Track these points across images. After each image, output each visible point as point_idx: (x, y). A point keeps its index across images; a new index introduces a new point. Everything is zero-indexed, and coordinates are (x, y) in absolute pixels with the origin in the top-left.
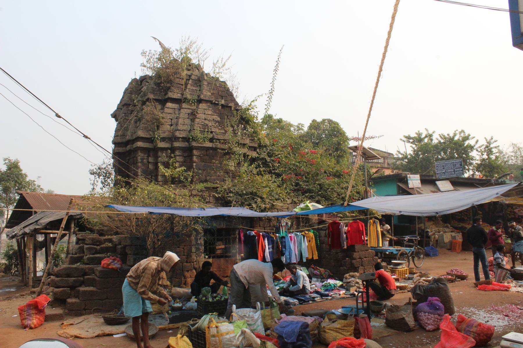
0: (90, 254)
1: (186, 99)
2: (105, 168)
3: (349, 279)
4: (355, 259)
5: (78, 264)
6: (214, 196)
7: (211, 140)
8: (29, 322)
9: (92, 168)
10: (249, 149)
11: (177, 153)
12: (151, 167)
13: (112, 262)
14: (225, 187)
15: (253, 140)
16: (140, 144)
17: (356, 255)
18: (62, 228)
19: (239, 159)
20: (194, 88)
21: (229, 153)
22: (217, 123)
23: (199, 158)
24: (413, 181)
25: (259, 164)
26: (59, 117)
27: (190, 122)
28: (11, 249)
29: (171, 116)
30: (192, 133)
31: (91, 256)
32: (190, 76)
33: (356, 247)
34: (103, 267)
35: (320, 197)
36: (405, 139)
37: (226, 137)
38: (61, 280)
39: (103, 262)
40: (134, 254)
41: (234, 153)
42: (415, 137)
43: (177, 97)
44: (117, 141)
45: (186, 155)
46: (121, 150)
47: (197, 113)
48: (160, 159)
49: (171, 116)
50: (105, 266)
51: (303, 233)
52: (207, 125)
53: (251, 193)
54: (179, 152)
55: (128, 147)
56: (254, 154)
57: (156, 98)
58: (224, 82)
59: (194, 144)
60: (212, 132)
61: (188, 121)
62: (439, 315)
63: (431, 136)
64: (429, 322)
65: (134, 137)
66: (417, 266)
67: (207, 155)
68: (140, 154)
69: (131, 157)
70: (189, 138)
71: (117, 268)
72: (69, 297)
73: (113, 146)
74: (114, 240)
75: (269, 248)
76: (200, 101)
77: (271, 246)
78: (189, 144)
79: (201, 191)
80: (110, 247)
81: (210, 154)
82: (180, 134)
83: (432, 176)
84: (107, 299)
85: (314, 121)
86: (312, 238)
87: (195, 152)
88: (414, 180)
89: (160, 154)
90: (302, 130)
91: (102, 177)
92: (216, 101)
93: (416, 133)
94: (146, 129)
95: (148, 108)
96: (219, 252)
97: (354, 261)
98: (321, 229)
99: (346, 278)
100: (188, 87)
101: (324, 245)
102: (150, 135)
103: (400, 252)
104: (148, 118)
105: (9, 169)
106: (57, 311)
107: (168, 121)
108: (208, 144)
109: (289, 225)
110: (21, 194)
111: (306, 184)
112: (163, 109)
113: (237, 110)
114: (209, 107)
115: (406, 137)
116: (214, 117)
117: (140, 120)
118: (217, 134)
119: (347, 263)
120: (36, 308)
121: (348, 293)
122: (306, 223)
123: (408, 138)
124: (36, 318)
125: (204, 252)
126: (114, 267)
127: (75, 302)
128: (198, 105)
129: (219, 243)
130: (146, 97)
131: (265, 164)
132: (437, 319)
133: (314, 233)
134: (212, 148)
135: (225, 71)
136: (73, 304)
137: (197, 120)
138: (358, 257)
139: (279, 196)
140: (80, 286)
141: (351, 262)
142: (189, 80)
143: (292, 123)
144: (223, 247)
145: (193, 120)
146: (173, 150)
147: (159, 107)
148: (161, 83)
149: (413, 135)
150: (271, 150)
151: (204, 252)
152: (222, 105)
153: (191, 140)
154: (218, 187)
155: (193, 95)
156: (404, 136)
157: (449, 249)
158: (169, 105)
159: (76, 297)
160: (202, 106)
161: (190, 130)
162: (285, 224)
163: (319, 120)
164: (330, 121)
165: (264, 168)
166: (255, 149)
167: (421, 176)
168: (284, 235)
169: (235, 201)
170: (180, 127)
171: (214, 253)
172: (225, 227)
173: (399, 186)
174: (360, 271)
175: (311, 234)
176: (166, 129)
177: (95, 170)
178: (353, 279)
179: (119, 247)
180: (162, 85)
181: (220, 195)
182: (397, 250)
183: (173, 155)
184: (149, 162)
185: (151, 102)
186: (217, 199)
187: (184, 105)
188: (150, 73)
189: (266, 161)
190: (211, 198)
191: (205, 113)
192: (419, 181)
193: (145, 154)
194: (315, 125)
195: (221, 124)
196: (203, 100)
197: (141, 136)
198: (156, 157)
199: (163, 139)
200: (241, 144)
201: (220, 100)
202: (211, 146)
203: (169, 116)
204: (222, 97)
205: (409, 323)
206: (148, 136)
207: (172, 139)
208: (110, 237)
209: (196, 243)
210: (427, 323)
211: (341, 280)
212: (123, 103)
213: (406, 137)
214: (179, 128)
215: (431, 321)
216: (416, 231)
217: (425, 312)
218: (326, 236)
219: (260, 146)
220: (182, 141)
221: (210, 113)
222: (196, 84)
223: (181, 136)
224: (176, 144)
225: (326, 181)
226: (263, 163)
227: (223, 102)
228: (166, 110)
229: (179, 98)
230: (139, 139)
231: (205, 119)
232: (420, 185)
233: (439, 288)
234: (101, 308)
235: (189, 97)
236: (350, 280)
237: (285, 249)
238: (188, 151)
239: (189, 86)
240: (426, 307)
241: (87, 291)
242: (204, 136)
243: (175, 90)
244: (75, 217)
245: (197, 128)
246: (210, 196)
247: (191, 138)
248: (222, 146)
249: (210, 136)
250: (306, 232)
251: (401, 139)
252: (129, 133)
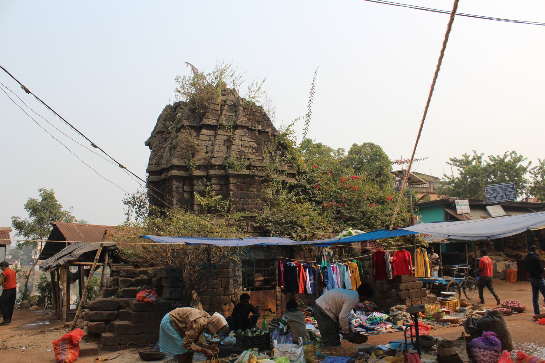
0: (125, 287)
1: (221, 125)
2: (139, 198)
3: (396, 312)
4: (402, 290)
5: (113, 297)
6: (252, 226)
7: (248, 167)
8: (64, 357)
9: (126, 197)
10: (287, 176)
11: (213, 181)
12: (186, 195)
13: (147, 295)
14: (264, 216)
15: (291, 166)
16: (175, 172)
17: (402, 286)
18: (97, 259)
19: (278, 187)
20: (230, 114)
21: (267, 181)
22: (254, 150)
23: (237, 186)
24: (462, 207)
25: (298, 191)
26: (95, 147)
27: (226, 149)
28: (45, 282)
29: (208, 143)
30: (228, 161)
31: (126, 288)
32: (225, 101)
33: (402, 278)
34: (139, 301)
35: (362, 225)
36: (451, 162)
37: (264, 164)
38: (96, 314)
39: (138, 295)
40: (170, 287)
41: (272, 181)
42: (462, 160)
43: (212, 124)
44: (151, 170)
45: (223, 183)
46: (155, 178)
47: (233, 139)
48: (195, 187)
49: (208, 143)
50: (141, 299)
51: (346, 263)
52: (244, 152)
53: (291, 222)
54: (215, 180)
55: (163, 176)
56: (293, 181)
57: (191, 124)
58: (261, 107)
59: (231, 172)
60: (249, 159)
61: (224, 148)
62: (496, 351)
63: (479, 158)
64: (485, 359)
65: (169, 166)
66: (469, 297)
67: (244, 183)
68: (175, 182)
69: (167, 185)
70: (226, 166)
71: (153, 301)
72: (103, 332)
73: (147, 174)
74: (150, 272)
75: (310, 280)
76: (236, 127)
77: (312, 278)
78: (226, 172)
79: (239, 220)
80: (145, 279)
81: (247, 181)
82: (216, 161)
83: (482, 201)
84: (141, 333)
85: (354, 145)
86: (356, 269)
87: (232, 180)
88: (463, 206)
89: (195, 182)
90: (343, 154)
91: (136, 207)
92: (252, 126)
93: (463, 156)
94: (181, 157)
95: (182, 136)
96: (257, 284)
97: (401, 293)
98: (365, 259)
99: (393, 311)
100: (224, 113)
101: (368, 276)
103: (450, 282)
104: (183, 145)
105: (44, 199)
106: (92, 346)
107: (203, 148)
108: (246, 172)
109: (331, 255)
110: (55, 225)
111: (348, 211)
112: (198, 136)
113: (275, 136)
114: (245, 133)
115: (452, 160)
116: (251, 143)
117: (174, 147)
118: (254, 161)
119: (394, 295)
120: (70, 342)
121: (395, 327)
122: (349, 253)
123: (455, 161)
124: (71, 353)
125: (243, 284)
126: (150, 300)
127: (110, 337)
128: (234, 131)
129: (258, 274)
130: (181, 124)
131: (305, 191)
132: (494, 355)
133: (357, 263)
134: (249, 176)
135: (261, 95)
136: (107, 338)
137: (233, 147)
138: (405, 288)
139: (320, 225)
140: (115, 320)
141: (397, 294)
142: (224, 105)
143: (331, 147)
144: (262, 278)
145: (229, 147)
146: (209, 178)
147: (194, 134)
148: (195, 109)
149: (460, 158)
150: (310, 176)
151: (243, 284)
152: (259, 131)
153: (227, 168)
154: (256, 217)
155: (229, 121)
156: (450, 159)
157: (503, 279)
158: (204, 131)
159: (110, 331)
160: (239, 132)
161: (227, 157)
162: (326, 254)
163: (360, 144)
164: (371, 145)
165: (304, 196)
166: (294, 176)
167: (469, 201)
168: (326, 265)
169: (274, 231)
170: (216, 154)
171: (253, 285)
172: (263, 258)
173: (446, 213)
174: (407, 303)
175: (355, 264)
176: (201, 157)
177: (129, 200)
178: (400, 312)
179: (155, 279)
180: (197, 111)
181: (258, 225)
182: (446, 281)
183: (209, 184)
184: (184, 191)
185: (185, 129)
186: (255, 229)
187: (220, 132)
188: (183, 99)
189: (305, 188)
190: (249, 228)
191: (242, 141)
192: (468, 207)
193: (180, 182)
194: (356, 150)
195: (258, 150)
196: (239, 126)
197: (176, 164)
198: (192, 186)
199: (199, 167)
200: (279, 171)
201: (257, 125)
202: (248, 173)
203: (204, 144)
204: (259, 122)
205: (463, 360)
206: (183, 164)
207: (208, 166)
208: (145, 269)
209: (234, 274)
210: (482, 360)
211: (388, 313)
212: (157, 130)
213: (452, 160)
214: (215, 155)
215: (487, 358)
216: (466, 260)
217: (480, 348)
218: (370, 267)
219: (299, 173)
220: (218, 169)
221: (246, 139)
222: (232, 109)
223: (217, 164)
224: (212, 172)
225: (370, 208)
226: (302, 191)
227: (260, 128)
228: (201, 137)
229: (214, 124)
230: (174, 167)
231: (242, 146)
232: (469, 211)
233: (495, 322)
234: (136, 343)
235: (225, 123)
236: (397, 313)
237: (328, 279)
238: (225, 179)
239: (224, 112)
240: (481, 342)
241: (122, 325)
242: (241, 163)
243: (211, 117)
245: (233, 154)
246: (248, 226)
247: (227, 165)
248: (260, 174)
249: (248, 163)
250: (349, 262)
251: (447, 163)
252: (163, 162)
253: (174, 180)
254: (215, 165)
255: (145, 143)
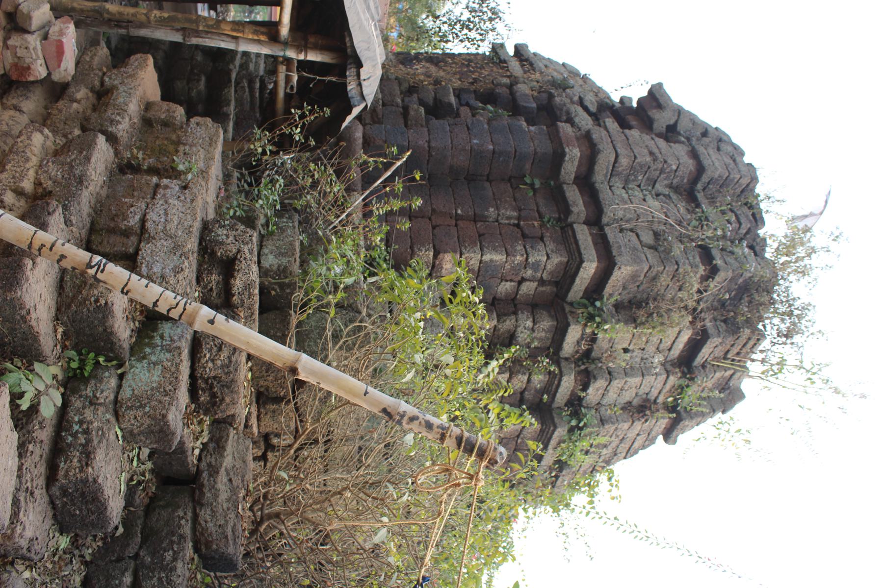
12: (506, 287)
16: (589, 269)
55: (573, 195)
59: (561, 432)
61: (627, 396)
65: (611, 233)
68: (556, 260)
89: (546, 324)
102: (611, 295)
170: (617, 384)
184: (523, 280)
193: (551, 273)
198: (534, 306)
206: (608, 290)
224: (568, 384)
230: (608, 266)
244: (350, 73)
247: (581, 425)
253: (565, 260)
254: (585, 388)
255: (660, 85)
